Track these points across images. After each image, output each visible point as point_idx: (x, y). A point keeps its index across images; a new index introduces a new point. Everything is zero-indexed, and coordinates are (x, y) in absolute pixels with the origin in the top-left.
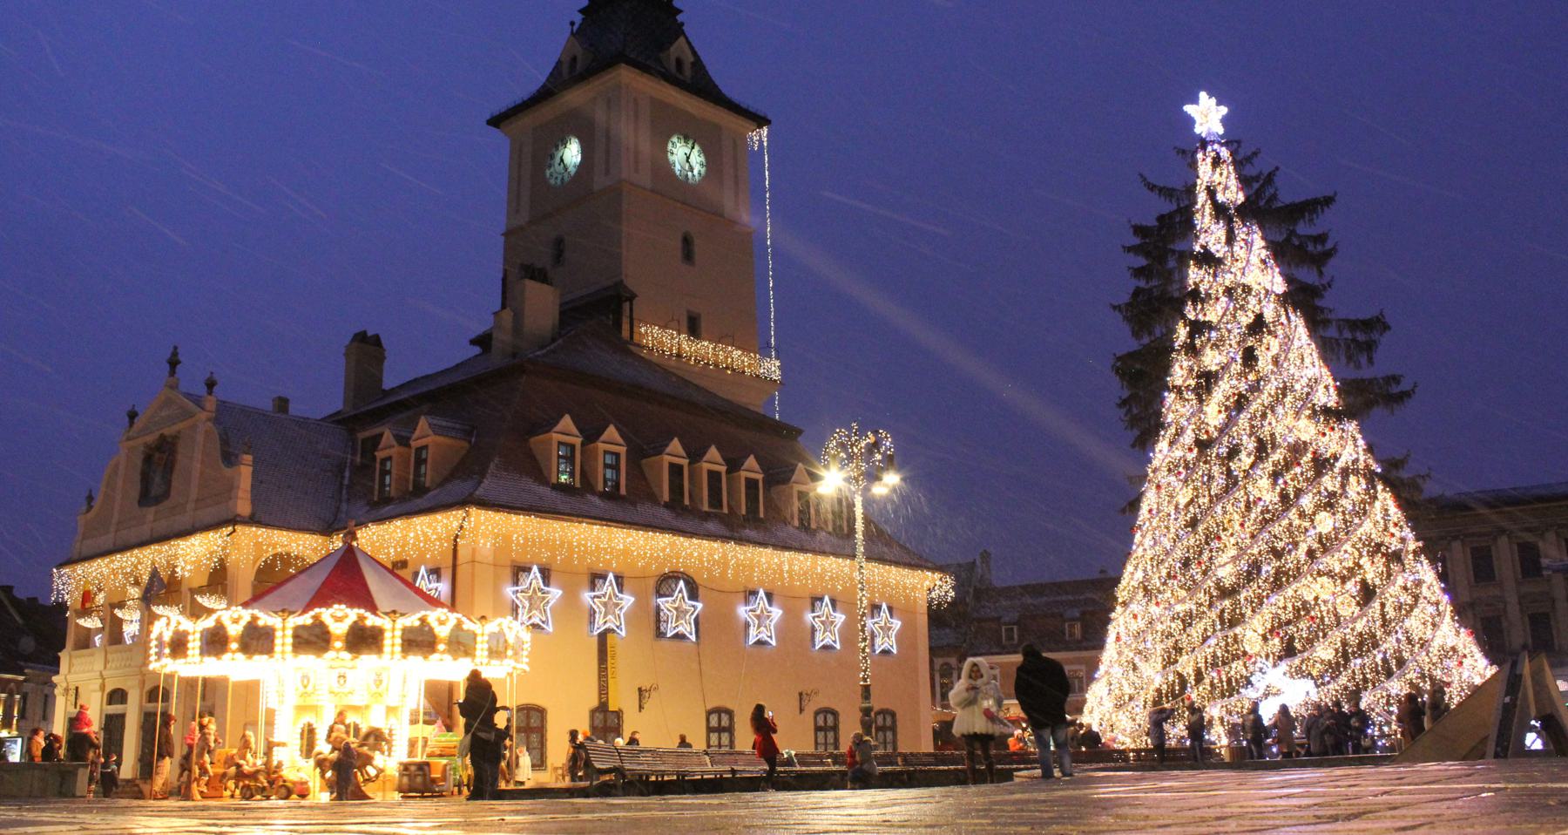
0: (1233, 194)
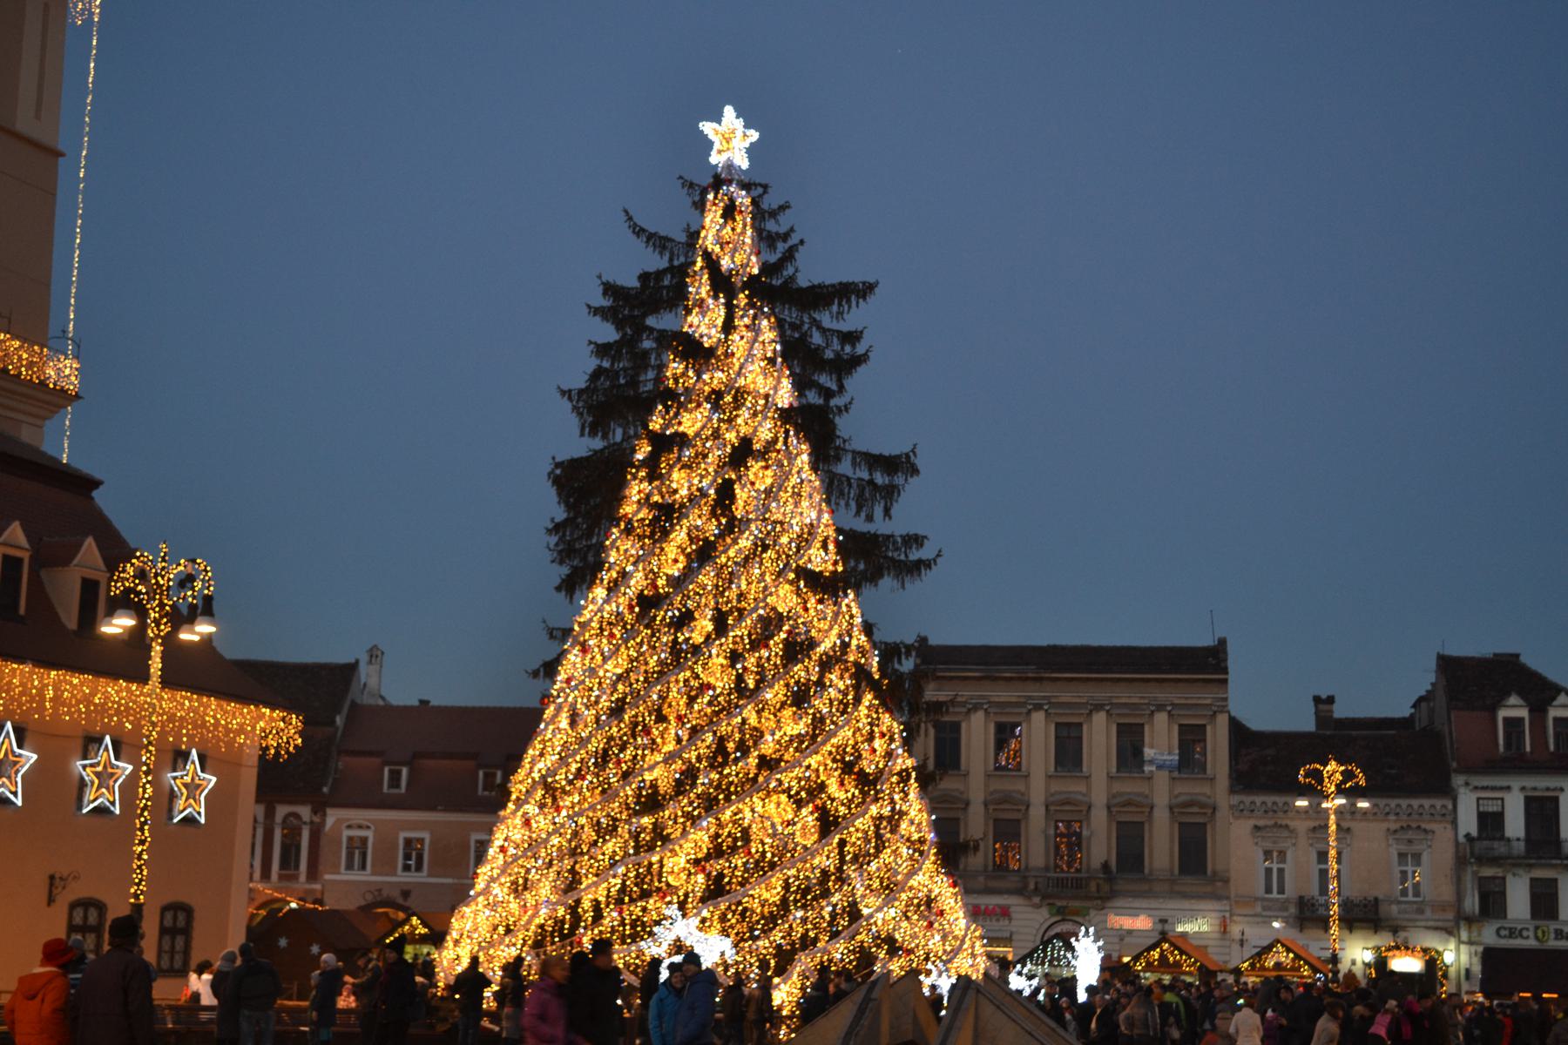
0: (742, 259)
